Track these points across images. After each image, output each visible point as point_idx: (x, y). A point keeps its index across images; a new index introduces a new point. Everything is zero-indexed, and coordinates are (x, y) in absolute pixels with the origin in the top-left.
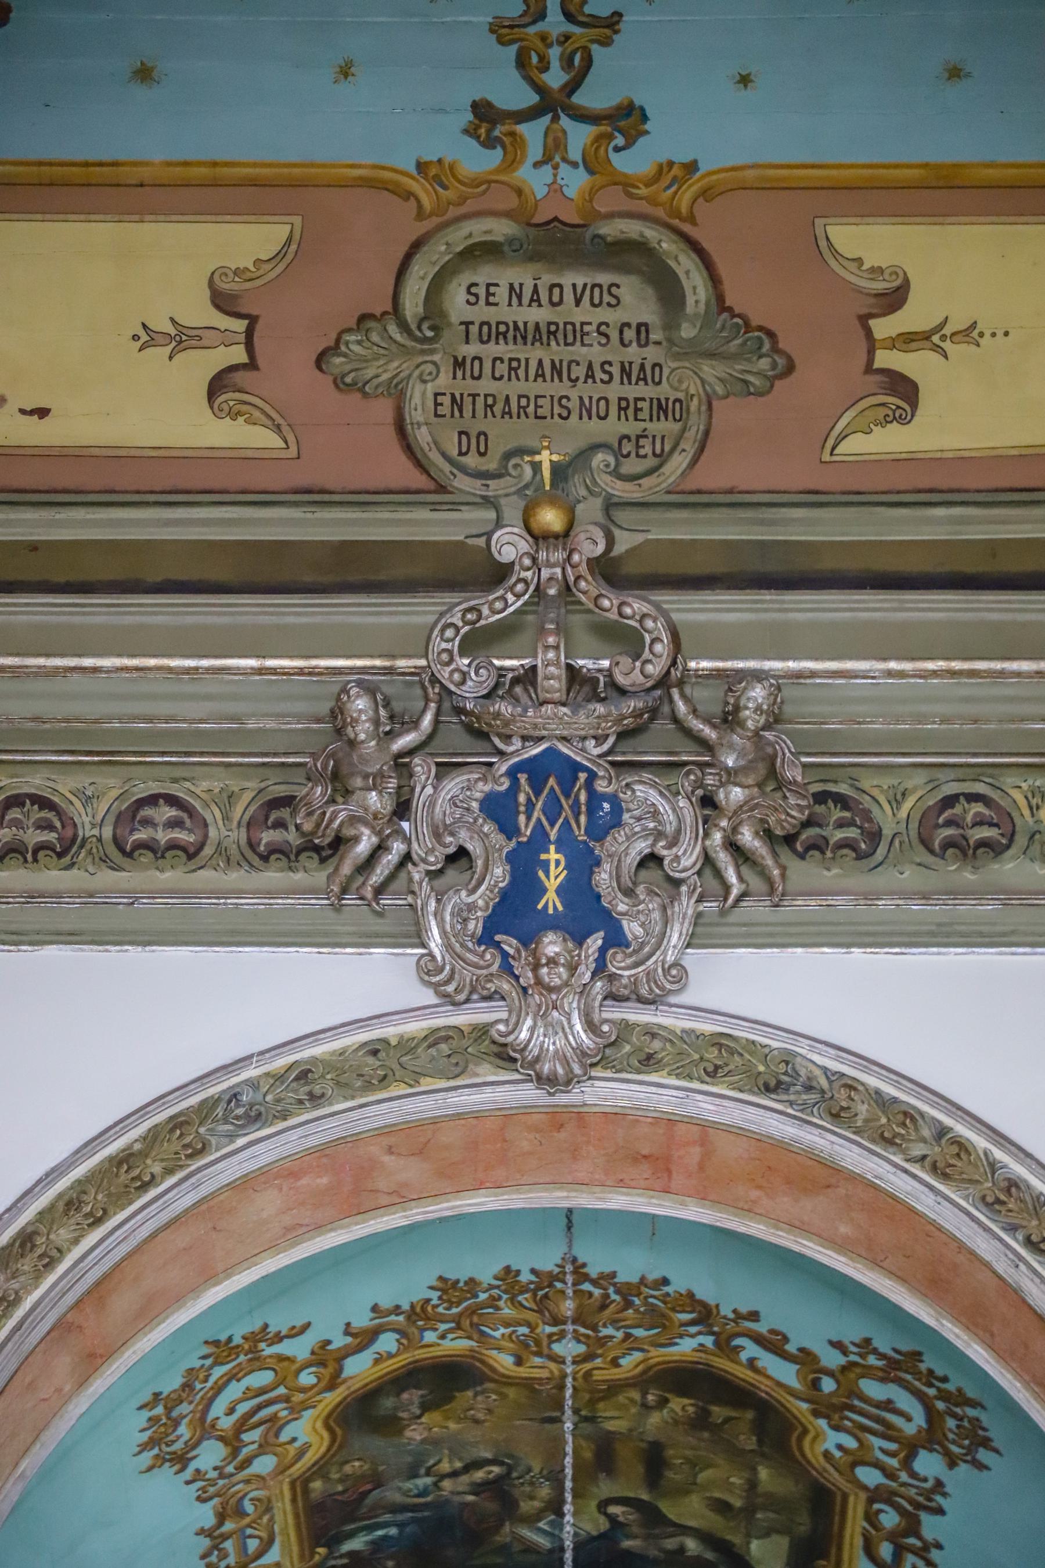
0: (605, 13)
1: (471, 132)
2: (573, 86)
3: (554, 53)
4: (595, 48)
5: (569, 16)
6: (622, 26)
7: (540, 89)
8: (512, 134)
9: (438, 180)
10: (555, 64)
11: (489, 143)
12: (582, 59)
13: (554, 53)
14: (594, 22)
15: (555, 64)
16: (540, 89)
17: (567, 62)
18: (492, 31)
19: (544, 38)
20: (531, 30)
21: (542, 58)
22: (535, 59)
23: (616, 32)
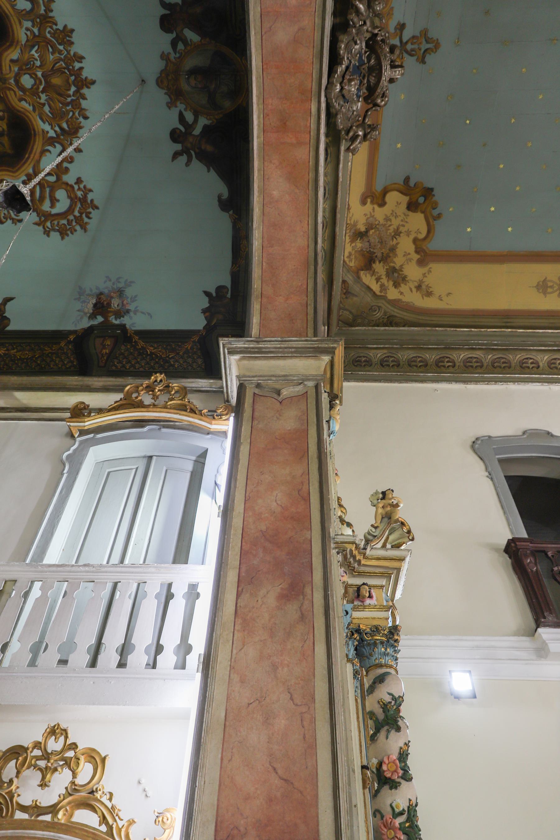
0: (426, 59)
1: (399, 24)
2: (407, 52)
3: (416, 46)
4: (415, 58)
5: (426, 50)
6: (421, 64)
7: (407, 43)
8: (397, 35)
9: (389, 13)
10: (413, 47)
11: (396, 28)
12: (413, 54)
13: (416, 46)
14: (424, 57)
15: (413, 47)
16: (407, 43)
17: (412, 50)
18: (424, 29)
19: (421, 43)
20: (424, 40)
21: (415, 43)
22: (415, 41)
23: (420, 63)
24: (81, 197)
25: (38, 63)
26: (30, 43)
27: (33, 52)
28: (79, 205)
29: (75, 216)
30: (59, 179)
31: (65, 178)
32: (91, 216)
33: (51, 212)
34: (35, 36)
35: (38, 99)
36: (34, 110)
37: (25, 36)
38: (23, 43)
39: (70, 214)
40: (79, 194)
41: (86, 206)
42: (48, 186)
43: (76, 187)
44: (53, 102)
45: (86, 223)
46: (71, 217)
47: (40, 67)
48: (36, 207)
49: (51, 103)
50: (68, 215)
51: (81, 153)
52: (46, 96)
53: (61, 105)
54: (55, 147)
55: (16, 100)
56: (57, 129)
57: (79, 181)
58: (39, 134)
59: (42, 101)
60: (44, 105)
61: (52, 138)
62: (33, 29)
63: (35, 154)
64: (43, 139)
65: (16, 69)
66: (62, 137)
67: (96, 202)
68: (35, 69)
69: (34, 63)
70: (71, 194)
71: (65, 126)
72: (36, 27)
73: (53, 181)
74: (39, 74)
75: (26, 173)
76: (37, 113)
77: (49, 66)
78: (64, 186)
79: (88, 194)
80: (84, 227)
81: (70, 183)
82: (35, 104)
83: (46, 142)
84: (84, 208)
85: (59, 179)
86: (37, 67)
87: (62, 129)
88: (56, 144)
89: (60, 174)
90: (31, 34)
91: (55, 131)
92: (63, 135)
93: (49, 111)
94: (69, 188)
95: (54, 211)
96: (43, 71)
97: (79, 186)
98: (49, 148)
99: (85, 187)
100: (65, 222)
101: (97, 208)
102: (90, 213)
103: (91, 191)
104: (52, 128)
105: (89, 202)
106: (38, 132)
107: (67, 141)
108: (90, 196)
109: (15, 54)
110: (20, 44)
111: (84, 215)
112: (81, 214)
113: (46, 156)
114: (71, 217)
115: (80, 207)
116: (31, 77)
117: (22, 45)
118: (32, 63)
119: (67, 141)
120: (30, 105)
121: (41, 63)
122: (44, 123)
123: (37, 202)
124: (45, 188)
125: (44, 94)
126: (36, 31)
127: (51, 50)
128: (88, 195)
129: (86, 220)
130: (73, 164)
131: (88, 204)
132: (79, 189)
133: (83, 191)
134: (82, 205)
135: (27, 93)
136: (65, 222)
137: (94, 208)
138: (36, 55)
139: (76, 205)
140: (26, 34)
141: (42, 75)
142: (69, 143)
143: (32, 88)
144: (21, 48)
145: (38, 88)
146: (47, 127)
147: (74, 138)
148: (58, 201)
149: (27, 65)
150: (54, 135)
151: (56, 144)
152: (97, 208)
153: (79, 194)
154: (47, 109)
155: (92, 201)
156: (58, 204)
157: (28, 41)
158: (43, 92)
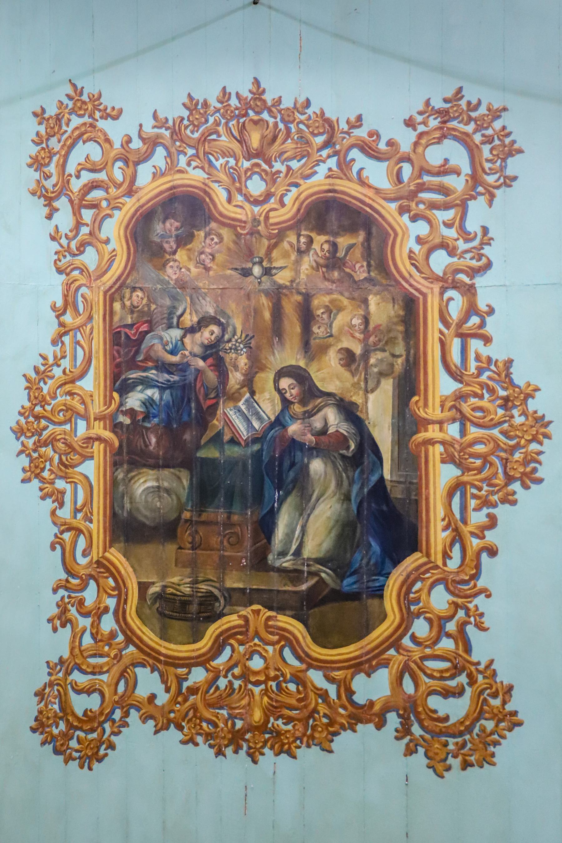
24: (439, 119)
25: (232, 162)
26: (206, 166)
27: (217, 164)
28: (454, 124)
29: (475, 131)
30: (407, 159)
31: (405, 147)
32: (474, 102)
33: (467, 175)
34: (197, 156)
35: (281, 175)
36: (297, 185)
37: (197, 169)
38: (206, 176)
39: (472, 140)
40: (434, 123)
41: (456, 111)
42: (420, 176)
43: (421, 128)
44: (286, 152)
45: (489, 110)
46: (478, 138)
47: (237, 161)
48: (458, 202)
49: (286, 156)
50: (474, 143)
51: (363, 117)
52: (276, 161)
53: (289, 141)
54: (353, 160)
55: (283, 211)
56: (325, 153)
57: (410, 123)
58: (333, 185)
59: (283, 169)
60: (289, 168)
61: (339, 164)
62: (188, 156)
63: (365, 196)
64: (341, 179)
65: (240, 198)
66: (338, 147)
67: (449, 94)
68: (239, 168)
69: (232, 168)
70: (434, 138)
71: (320, 140)
72: (185, 150)
73: (411, 168)
74: (247, 164)
75: (398, 214)
76: (301, 182)
77: (236, 146)
78: (420, 150)
79: (433, 107)
80: (496, 114)
81: (414, 139)
82: (288, 181)
83: (345, 175)
84: (458, 116)
85: (407, 159)
86: (236, 164)
87: (327, 144)
88: (349, 158)
89: (398, 156)
90: (194, 161)
91: (329, 157)
92: (334, 144)
93: (299, 161)
94: (423, 141)
95: (466, 169)
96: (241, 157)
97: (419, 124)
98: (355, 169)
99: (420, 113)
100: (486, 150)
101: (460, 89)
102: (469, 103)
103: (427, 103)
104: (324, 162)
105: (449, 105)
106: (330, 185)
107: (344, 138)
108: (437, 103)
109: (221, 195)
110: (207, 181)
111: (473, 114)
112: (470, 119)
113: (367, 177)
114: (478, 138)
115: (459, 122)
116: (250, 178)
117: (208, 178)
118: (231, 170)
119: (344, 138)
120: (290, 191)
121: (231, 156)
122: (316, 173)
123: (448, 198)
124: (424, 184)
125: (273, 163)
126: (191, 152)
127: (214, 137)
128: (436, 108)
129: (483, 110)
130: (381, 132)
131: (452, 107)
132: (425, 123)
133: (428, 117)
134: (455, 118)
135: (273, 190)
136: (486, 150)
137: (460, 95)
138: (222, 161)
139: (454, 129)
140: (194, 168)
141: (248, 160)
142: (348, 137)
143: (265, 181)
144: (212, 181)
145: (264, 171)
146: (322, 169)
147: (338, 127)
148: (446, 160)
149: (234, 180)
150: (335, 158)
151: (349, 158)
152: (460, 89)
153: (434, 123)
154: (295, 165)
155: (446, 101)
156: (453, 162)
157: (203, 168)
158: (271, 166)
